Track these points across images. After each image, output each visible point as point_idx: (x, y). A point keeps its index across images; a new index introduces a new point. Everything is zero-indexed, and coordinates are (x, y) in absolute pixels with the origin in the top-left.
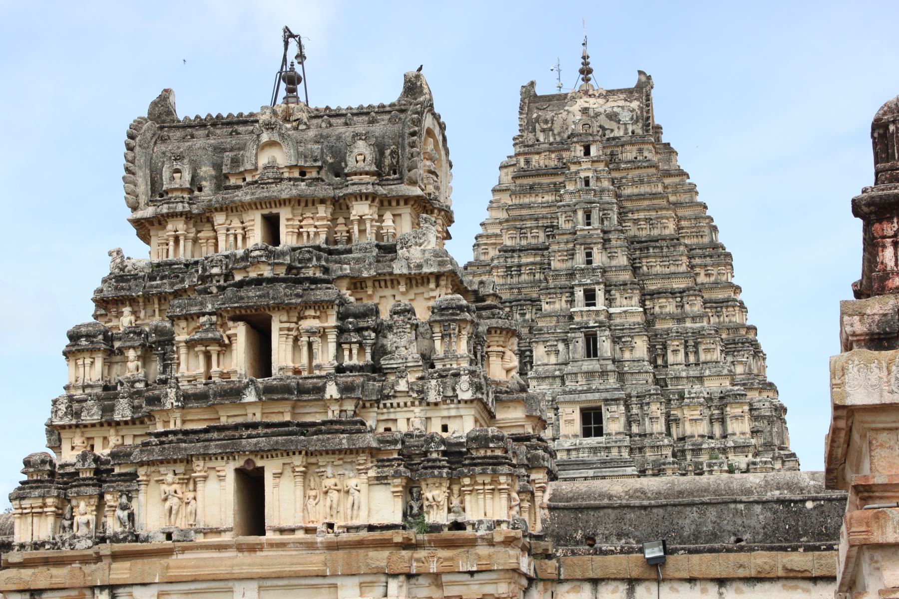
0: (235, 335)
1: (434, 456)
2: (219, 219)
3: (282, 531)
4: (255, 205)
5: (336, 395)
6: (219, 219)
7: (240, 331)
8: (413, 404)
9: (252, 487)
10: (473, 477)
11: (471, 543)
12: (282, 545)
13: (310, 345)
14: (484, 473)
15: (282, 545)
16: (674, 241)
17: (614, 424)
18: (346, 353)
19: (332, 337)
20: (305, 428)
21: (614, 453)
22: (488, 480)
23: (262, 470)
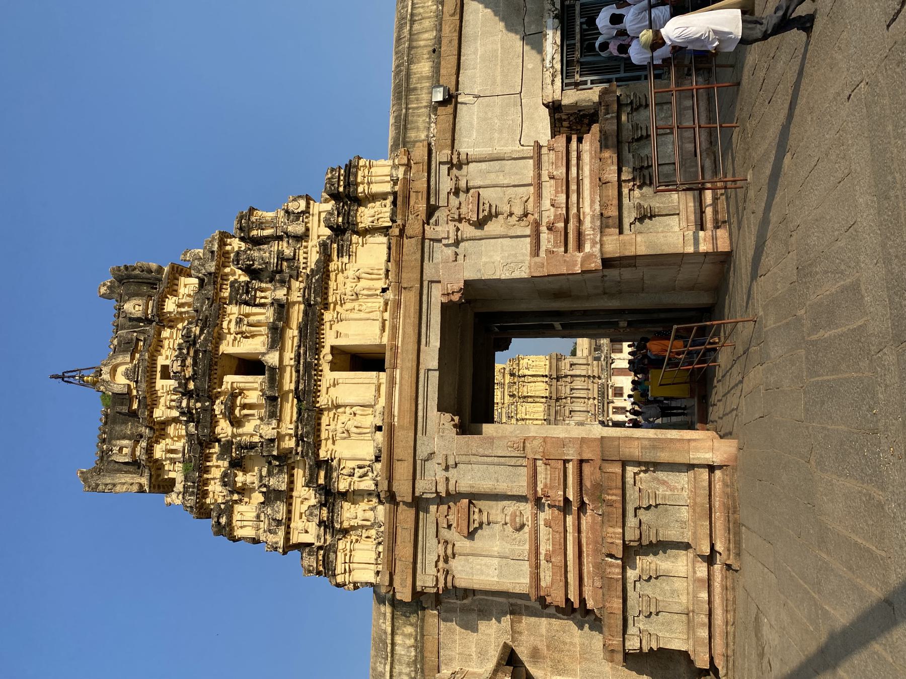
0: (232, 383)
1: (340, 219)
3: (383, 330)
4: (151, 383)
5: (284, 291)
7: (230, 380)
8: (306, 247)
10: (357, 184)
11: (407, 181)
12: (394, 328)
13: (249, 325)
14: (356, 176)
15: (394, 328)
18: (263, 301)
19: (247, 309)
22: (360, 173)
23: (332, 347)
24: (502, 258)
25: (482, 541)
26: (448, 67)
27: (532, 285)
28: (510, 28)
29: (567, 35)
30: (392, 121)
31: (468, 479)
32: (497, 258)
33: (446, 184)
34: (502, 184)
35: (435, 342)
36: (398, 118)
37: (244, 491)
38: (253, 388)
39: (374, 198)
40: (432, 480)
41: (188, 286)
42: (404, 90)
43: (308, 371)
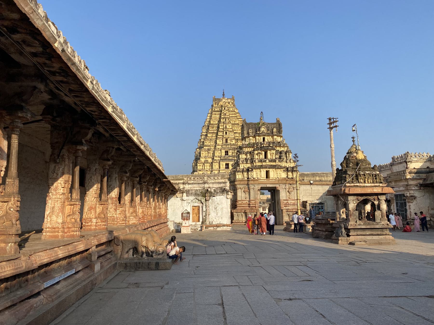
2: (257, 137)
6: (257, 137)
7: (263, 153)
9: (267, 173)
16: (238, 124)
17: (230, 154)
20: (274, 166)
21: (230, 158)
24: (283, 195)
25: (243, 193)
26: (317, 183)
27: (279, 200)
28: (324, 194)
29: (318, 204)
30: (308, 173)
31: (252, 192)
32: (283, 195)
33: (295, 186)
34: (293, 195)
35: (270, 186)
36: (309, 174)
37: (246, 154)
38: (262, 156)
39: (293, 174)
40: (251, 187)
41: (279, 139)
42: (314, 175)
43: (266, 168)
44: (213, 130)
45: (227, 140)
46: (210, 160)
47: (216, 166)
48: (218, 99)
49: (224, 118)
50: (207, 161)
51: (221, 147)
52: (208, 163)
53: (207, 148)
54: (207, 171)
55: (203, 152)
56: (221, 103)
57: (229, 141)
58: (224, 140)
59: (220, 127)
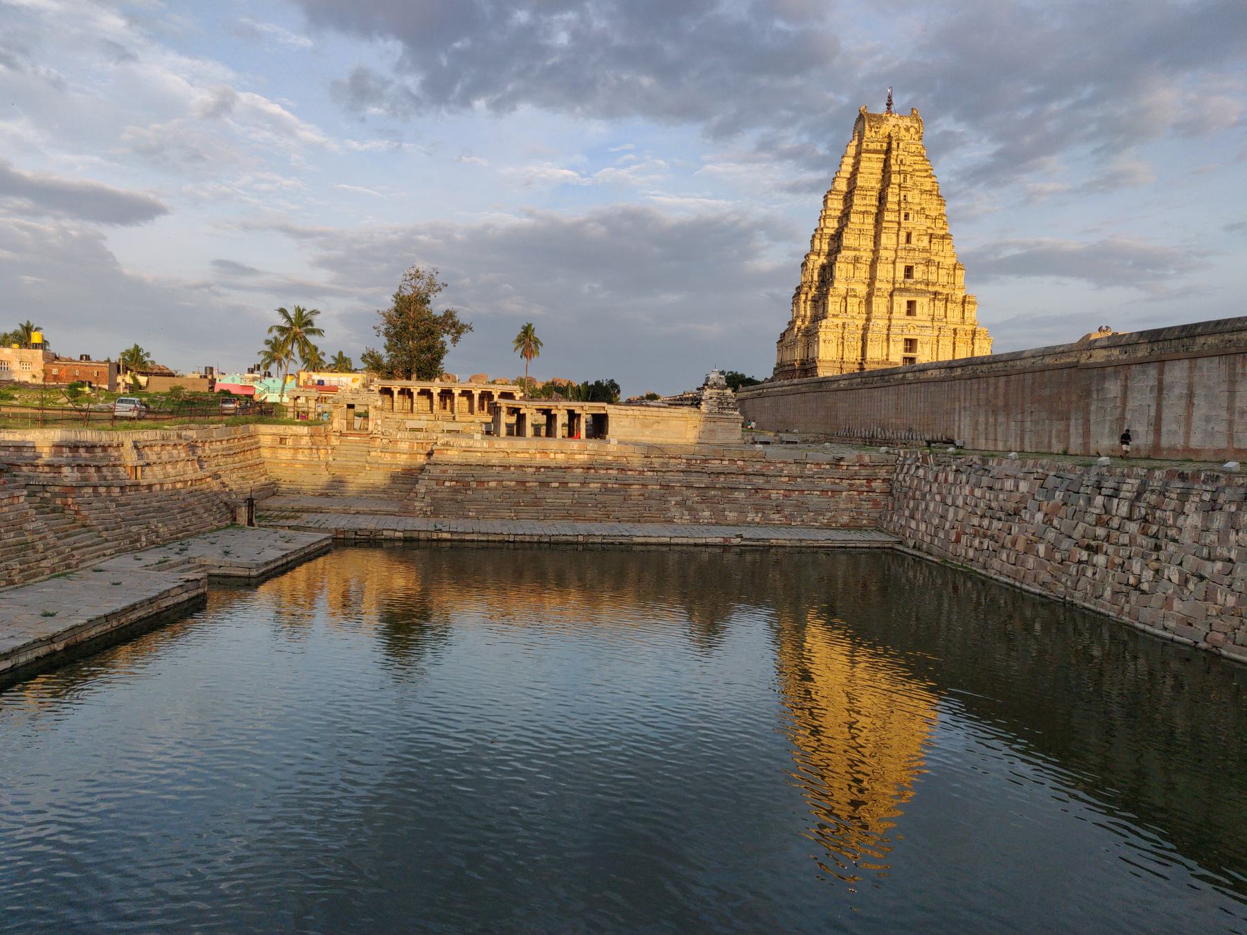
17: (918, 274)
21: (919, 287)
44: (865, 202)
45: (909, 236)
46: (862, 290)
47: (880, 305)
48: (874, 116)
49: (899, 173)
50: (853, 290)
51: (891, 255)
52: (855, 296)
53: (852, 254)
54: (853, 317)
55: (842, 266)
56: (886, 128)
57: (914, 240)
58: (903, 235)
59: (890, 199)
